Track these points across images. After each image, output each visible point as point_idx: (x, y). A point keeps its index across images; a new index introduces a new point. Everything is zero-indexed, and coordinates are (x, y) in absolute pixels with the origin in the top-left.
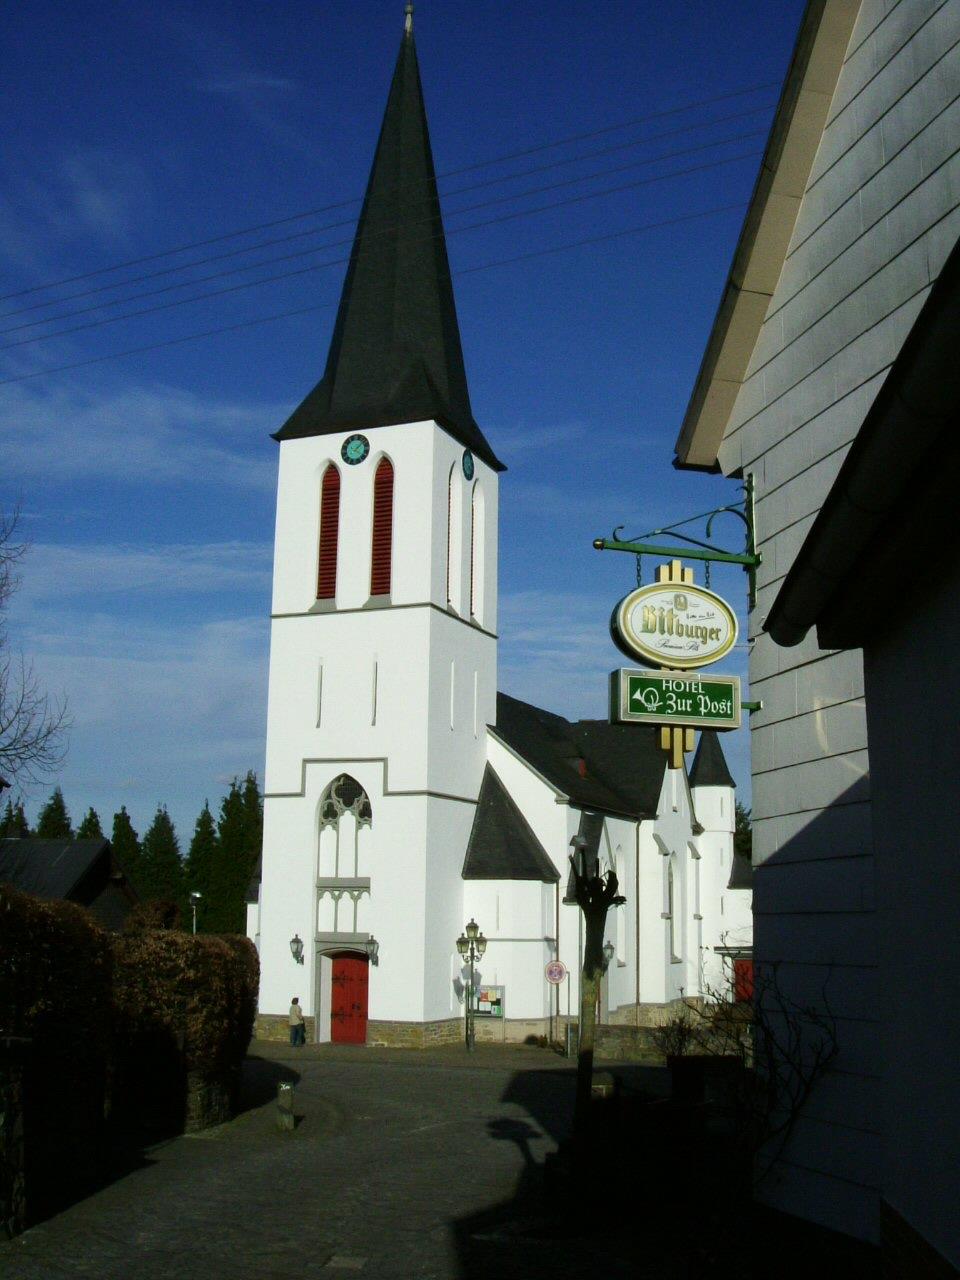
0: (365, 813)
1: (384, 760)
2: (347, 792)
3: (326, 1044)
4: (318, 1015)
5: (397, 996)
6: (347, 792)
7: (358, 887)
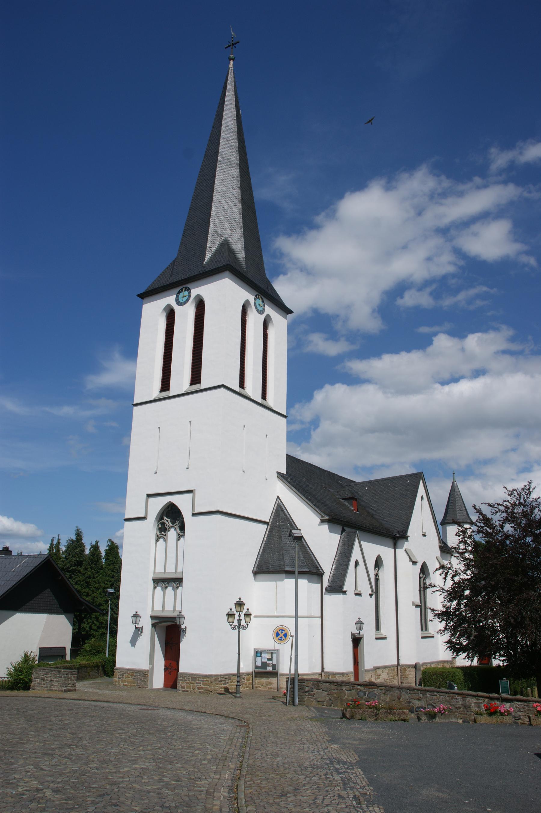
0: (182, 528)
1: (191, 491)
2: (171, 516)
3: (158, 690)
4: (152, 669)
5: (205, 654)
6: (171, 516)
7: (176, 581)
